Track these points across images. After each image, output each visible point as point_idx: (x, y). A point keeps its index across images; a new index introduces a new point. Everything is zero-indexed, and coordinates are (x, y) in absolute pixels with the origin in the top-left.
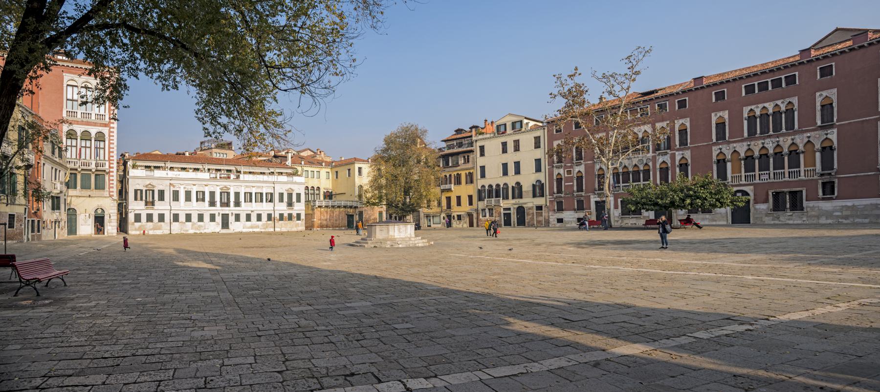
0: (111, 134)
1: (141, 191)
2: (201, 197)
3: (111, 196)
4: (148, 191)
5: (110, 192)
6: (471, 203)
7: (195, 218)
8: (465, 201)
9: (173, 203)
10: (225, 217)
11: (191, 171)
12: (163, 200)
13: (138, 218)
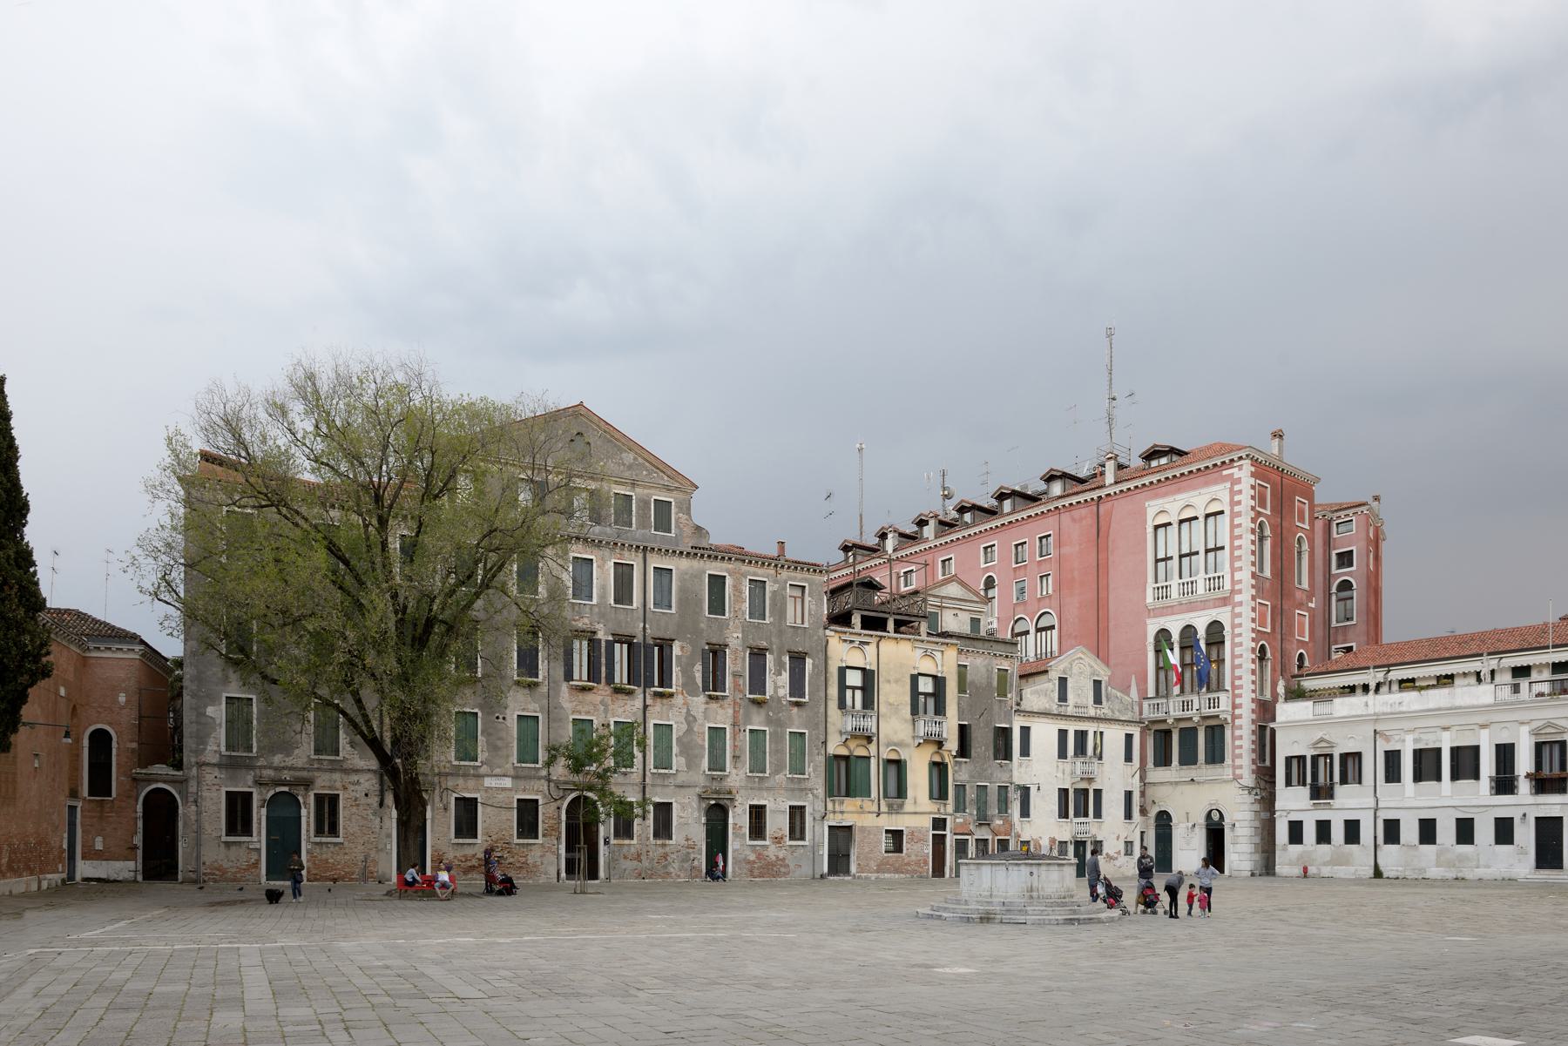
2: (1465, 763)
3: (1236, 778)
5: (1234, 767)
7: (1446, 831)
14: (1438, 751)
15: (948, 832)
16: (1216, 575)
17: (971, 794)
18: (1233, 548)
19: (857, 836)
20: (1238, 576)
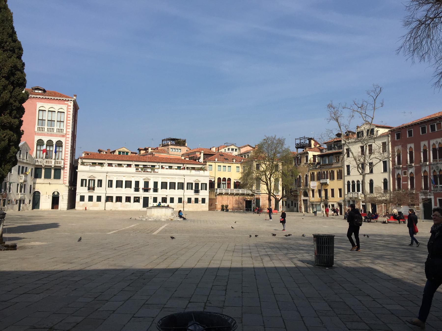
0: (67, 142)
1: (86, 180)
2: (128, 184)
3: (64, 183)
4: (91, 181)
5: (64, 180)
6: (341, 196)
8: (337, 193)
10: (146, 200)
11: (125, 166)
12: (102, 187)
13: (82, 199)
14: (122, 181)
16: (61, 128)
20: (68, 130)
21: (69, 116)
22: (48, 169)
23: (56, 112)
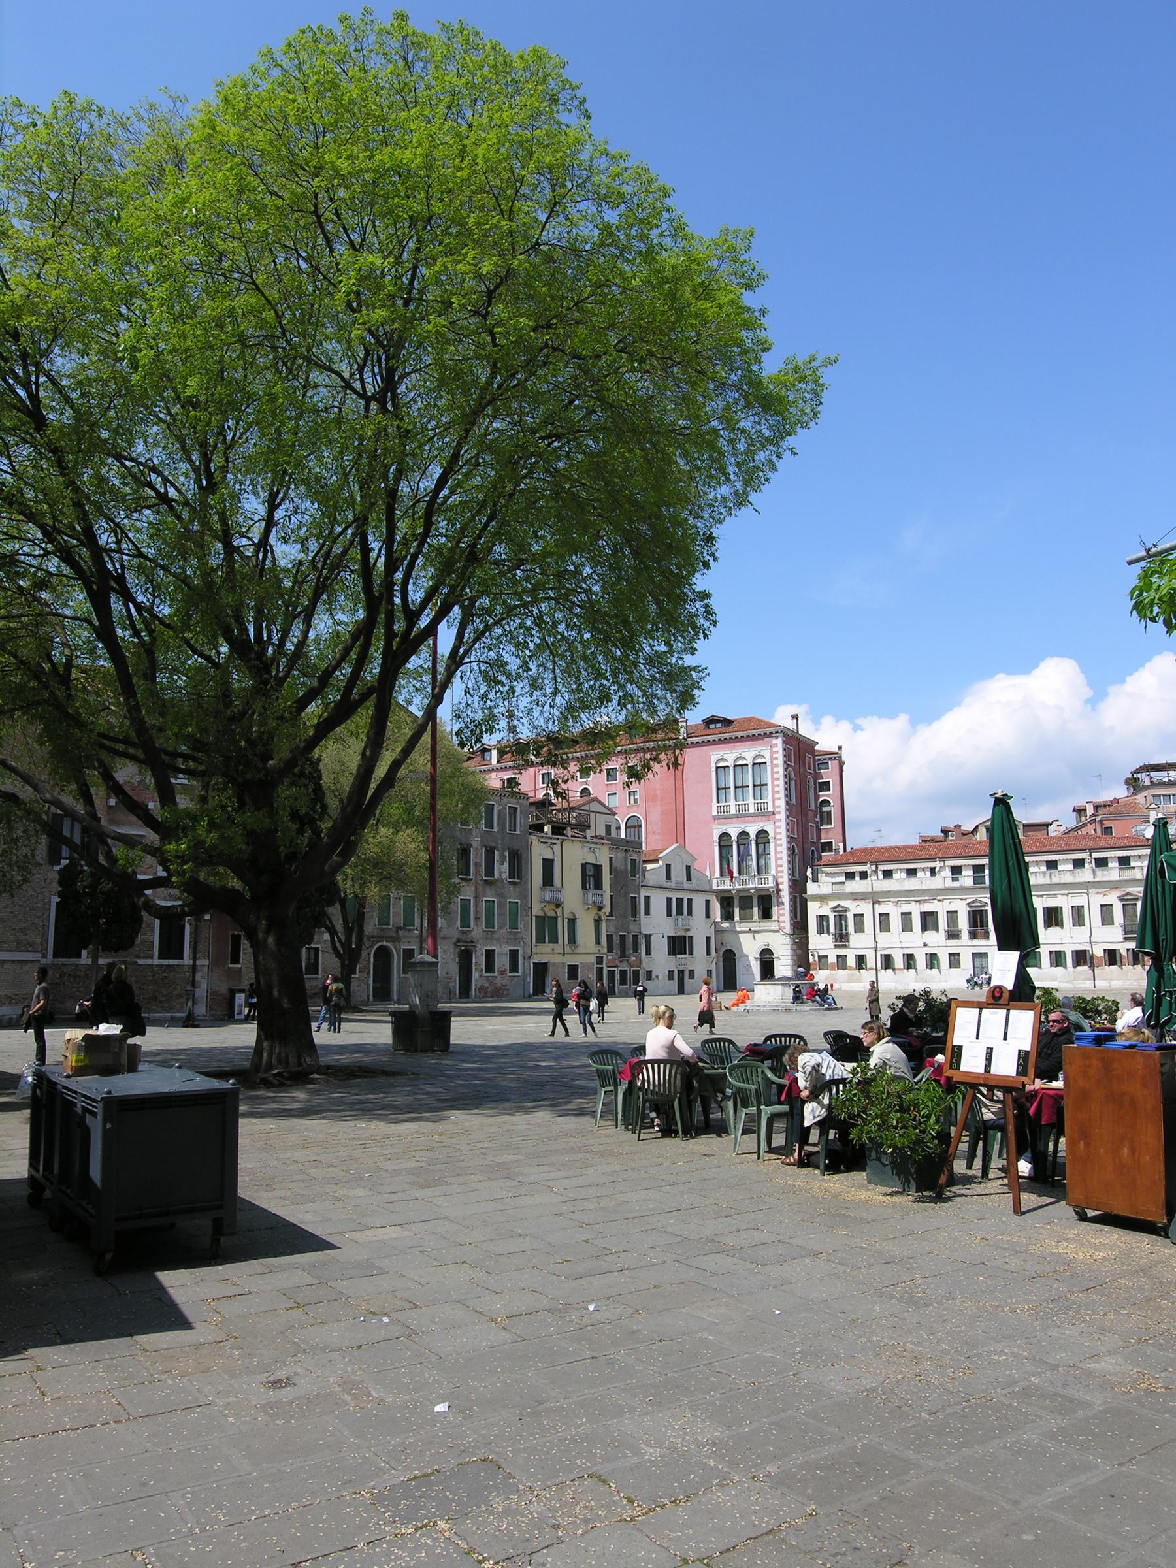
9: (883, 938)
15: (604, 966)
17: (616, 940)
18: (773, 786)
19: (551, 969)
21: (775, 770)
22: (746, 901)
23: (750, 766)
